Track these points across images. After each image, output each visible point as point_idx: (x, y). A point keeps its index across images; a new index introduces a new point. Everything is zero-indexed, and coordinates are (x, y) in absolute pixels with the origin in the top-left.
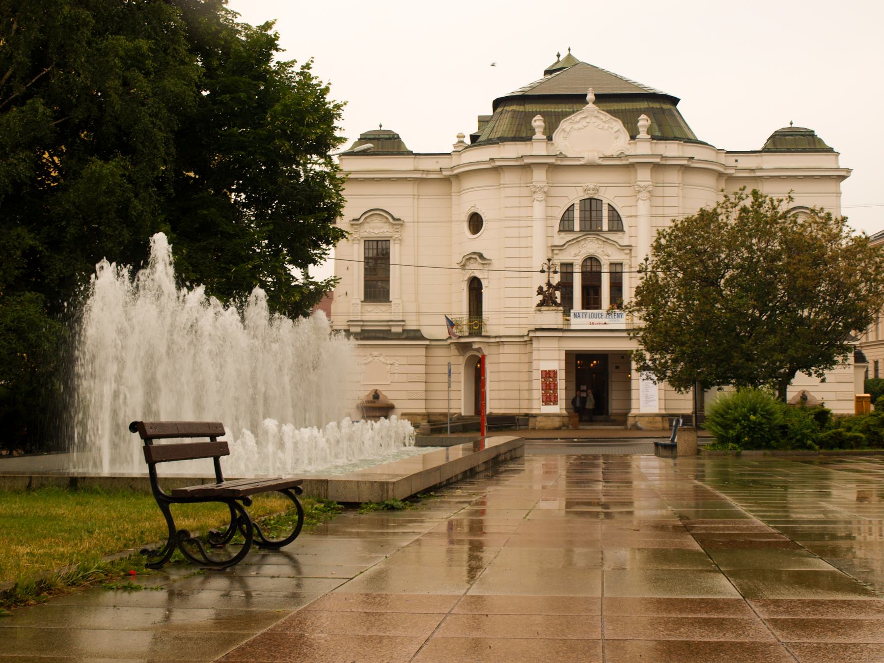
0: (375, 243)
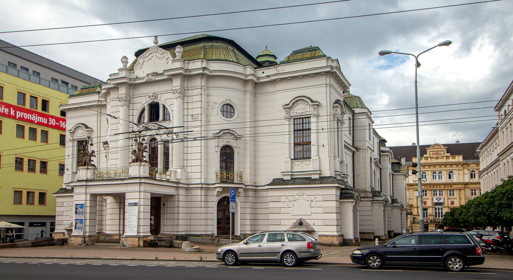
0: (301, 120)
